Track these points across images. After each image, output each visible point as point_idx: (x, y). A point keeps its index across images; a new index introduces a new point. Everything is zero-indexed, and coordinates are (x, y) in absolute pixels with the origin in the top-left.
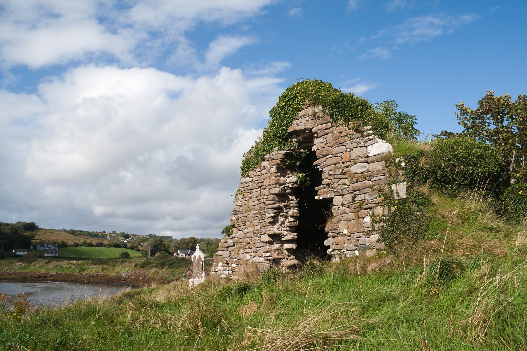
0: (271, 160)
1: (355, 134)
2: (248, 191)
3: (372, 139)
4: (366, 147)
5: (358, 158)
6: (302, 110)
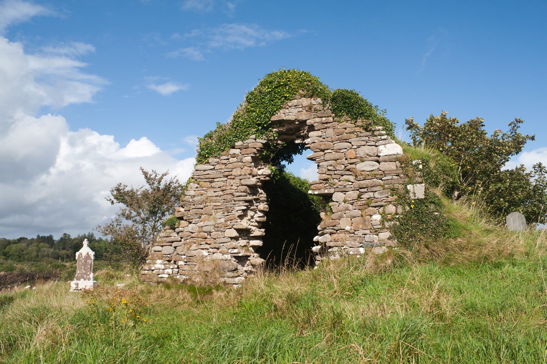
0: (245, 148)
1: (363, 132)
2: (208, 180)
3: (385, 140)
4: (376, 146)
5: (366, 156)
6: (293, 100)
